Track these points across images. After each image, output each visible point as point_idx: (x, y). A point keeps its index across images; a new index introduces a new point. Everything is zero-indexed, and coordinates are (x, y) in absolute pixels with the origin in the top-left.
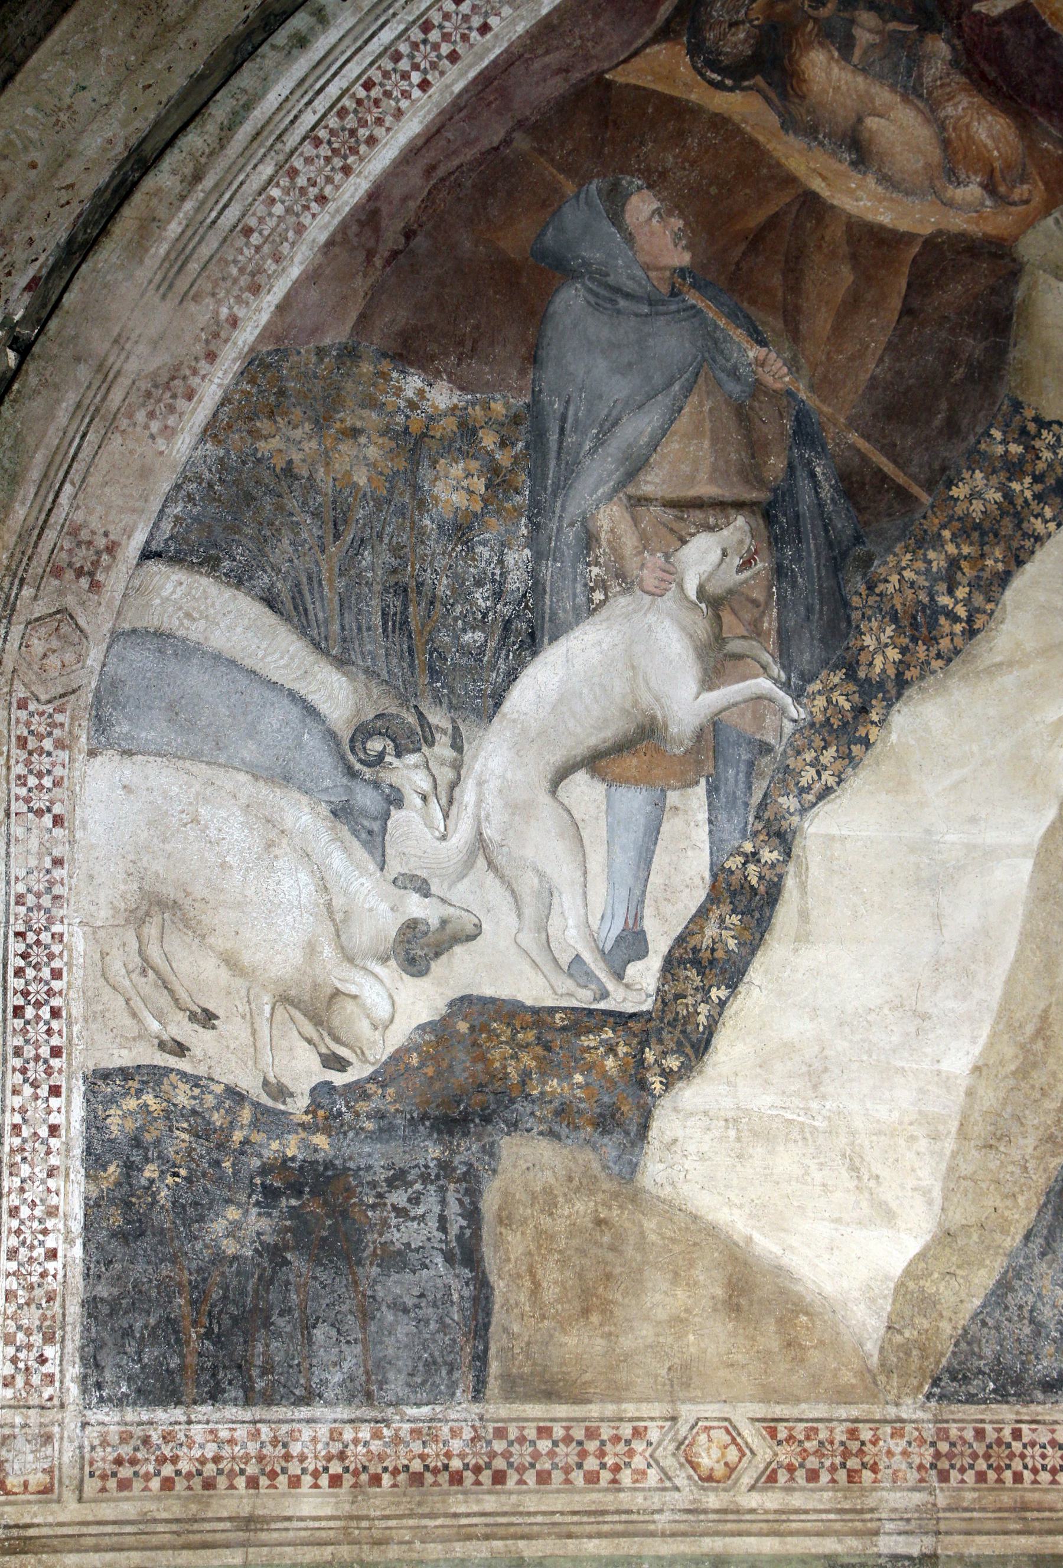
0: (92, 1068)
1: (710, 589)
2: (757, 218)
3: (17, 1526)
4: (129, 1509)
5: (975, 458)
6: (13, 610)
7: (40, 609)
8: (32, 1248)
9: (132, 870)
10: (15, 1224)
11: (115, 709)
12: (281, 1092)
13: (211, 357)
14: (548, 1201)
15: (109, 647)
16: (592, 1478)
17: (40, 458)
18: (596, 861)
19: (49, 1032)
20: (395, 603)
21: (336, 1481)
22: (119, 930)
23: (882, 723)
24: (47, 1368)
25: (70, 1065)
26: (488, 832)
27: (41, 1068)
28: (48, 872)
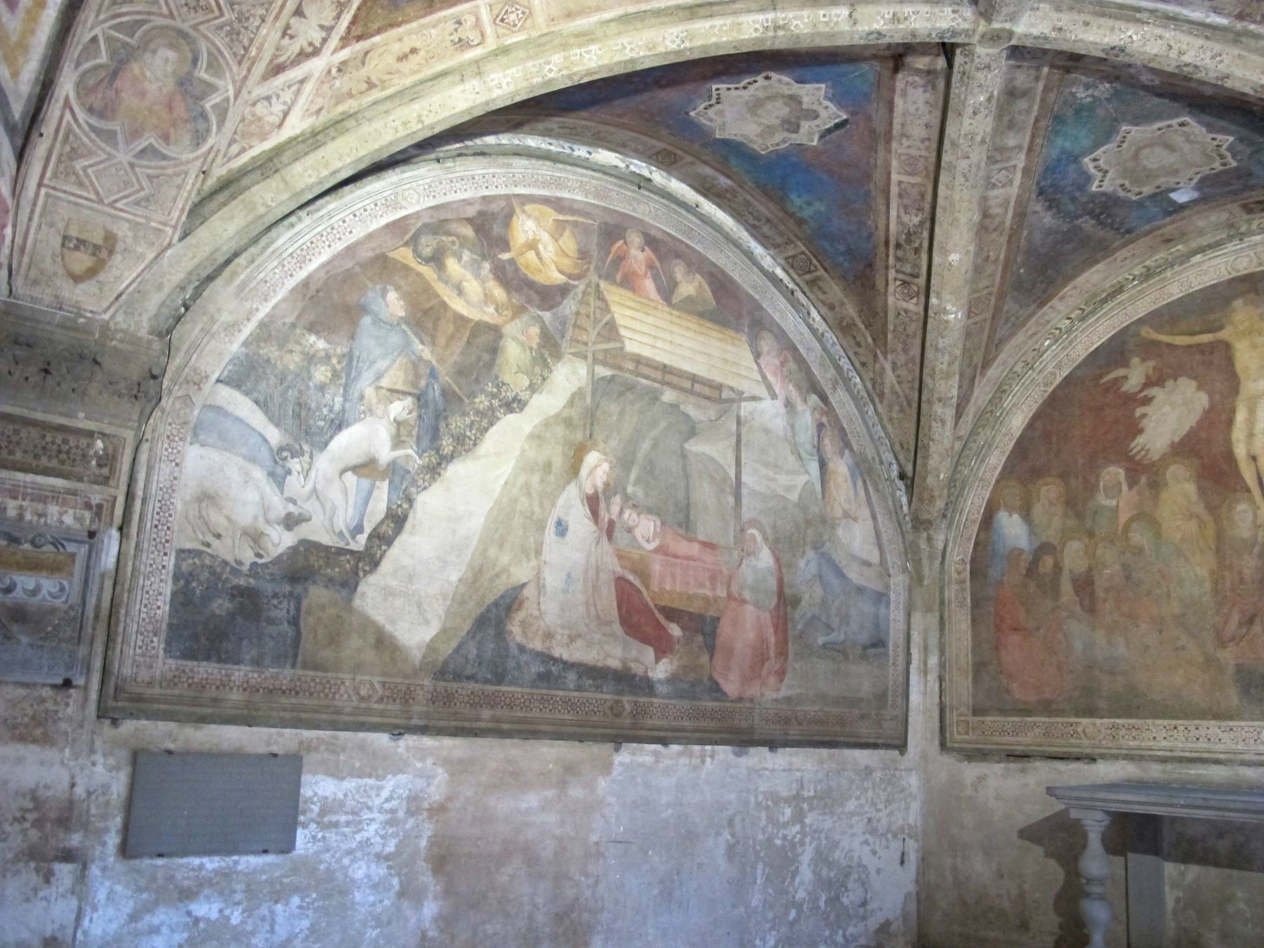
1: (399, 419)
2: (427, 306)
4: (176, 692)
5: (483, 391)
7: (180, 394)
12: (240, 563)
13: (248, 319)
14: (323, 607)
16: (327, 695)
17: (187, 344)
18: (351, 502)
20: (297, 409)
21: (245, 690)
23: (445, 469)
26: (318, 487)
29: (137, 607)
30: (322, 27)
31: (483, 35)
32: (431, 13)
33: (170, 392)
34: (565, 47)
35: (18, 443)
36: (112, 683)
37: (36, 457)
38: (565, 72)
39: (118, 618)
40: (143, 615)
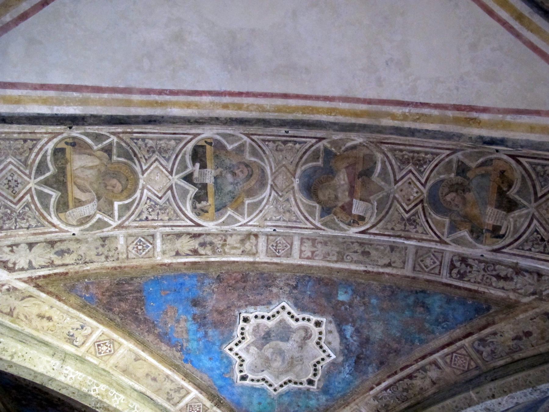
30: (30, 263)
31: (83, 343)
32: (78, 310)
34: (110, 384)
38: (100, 397)
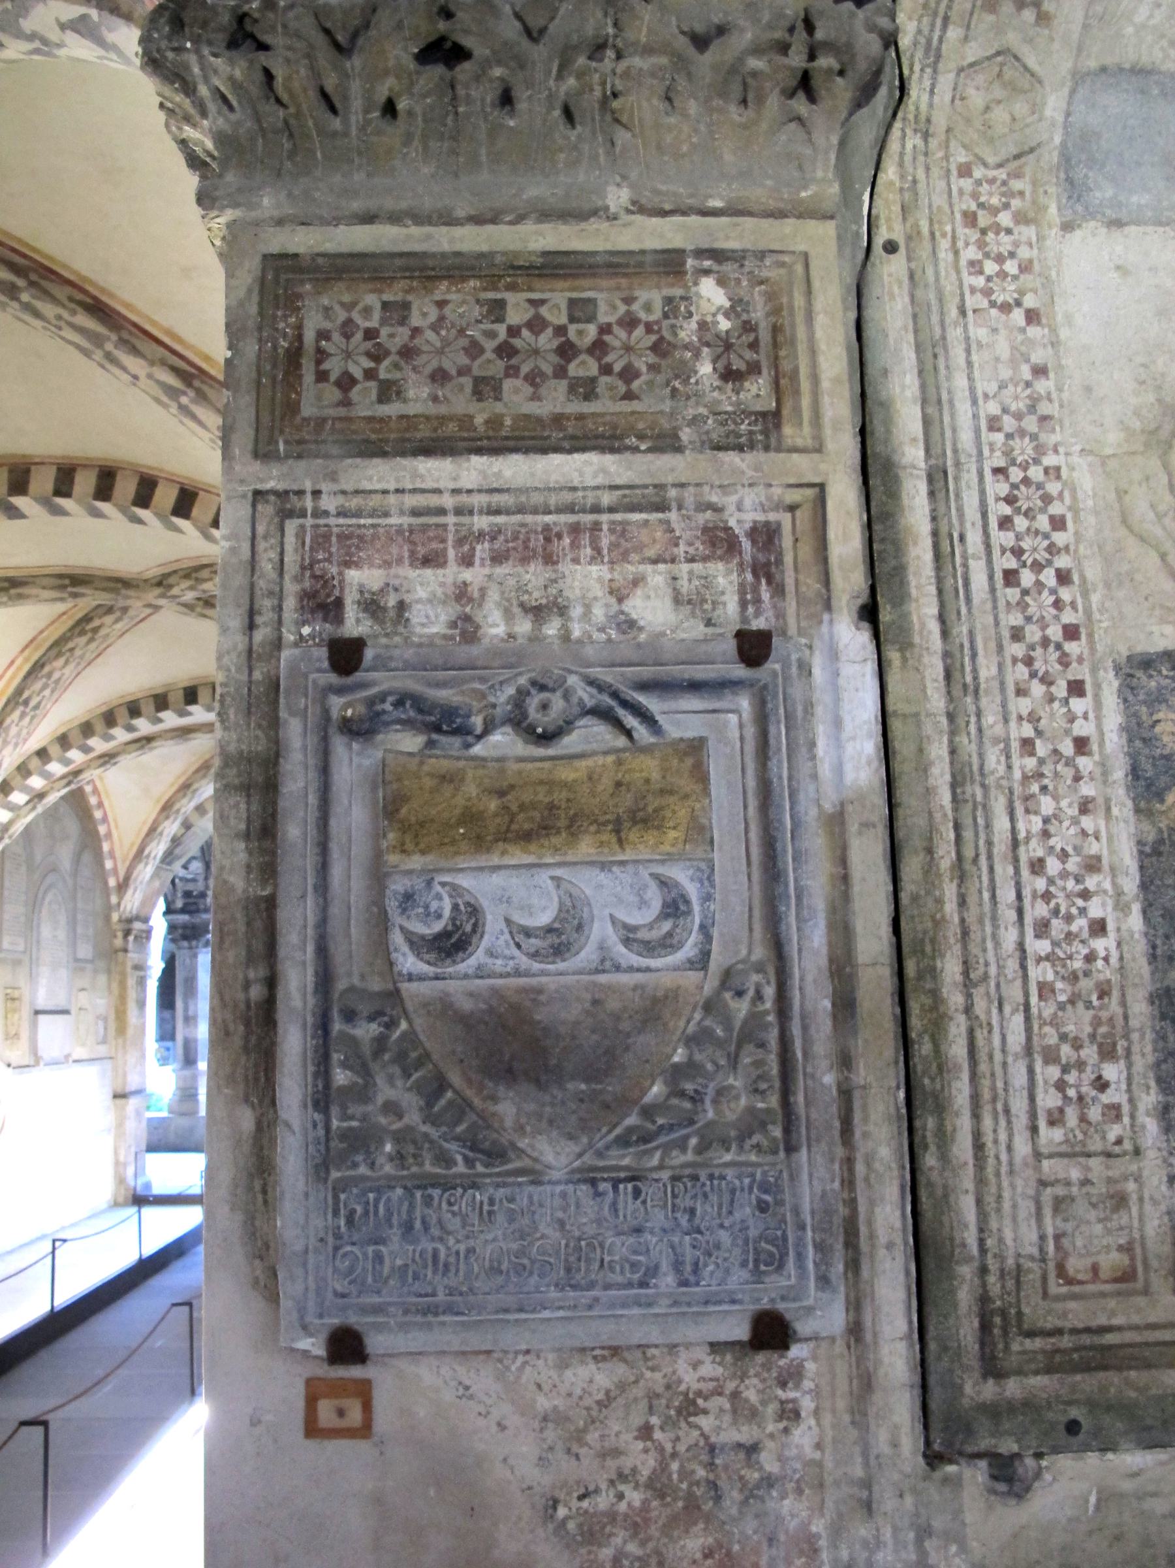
0: (1125, 653)
3: (1088, 1330)
6: (938, 56)
7: (973, 52)
8: (1069, 918)
9: (1143, 377)
10: (1041, 884)
11: (1091, 168)
15: (1073, 92)
19: (1058, 604)
22: (1139, 459)
24: (1106, 1098)
25: (1093, 650)
27: (1054, 655)
28: (1028, 384)
29: (1010, 937)
33: (935, 56)
35: (407, 353)
36: (965, 1296)
37: (485, 388)
39: (935, 994)
40: (1040, 973)
